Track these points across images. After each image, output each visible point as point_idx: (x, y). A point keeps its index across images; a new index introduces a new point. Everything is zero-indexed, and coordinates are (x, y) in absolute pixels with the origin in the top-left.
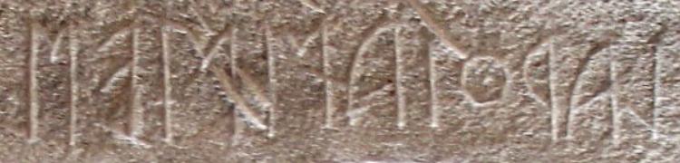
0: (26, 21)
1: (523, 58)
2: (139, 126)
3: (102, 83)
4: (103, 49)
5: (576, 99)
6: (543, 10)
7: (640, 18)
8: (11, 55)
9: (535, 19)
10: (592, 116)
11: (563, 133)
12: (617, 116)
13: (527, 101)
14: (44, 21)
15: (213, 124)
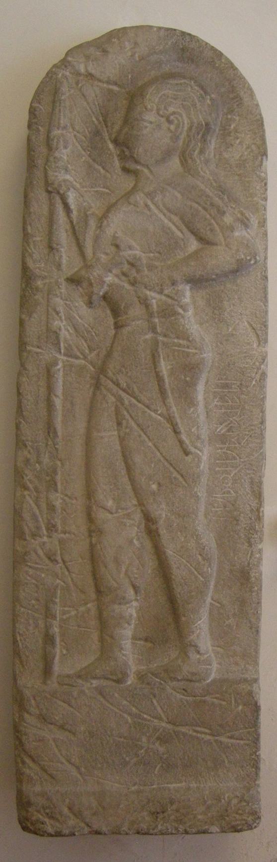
3: (227, 397)
9: (239, 492)
14: (241, 384)
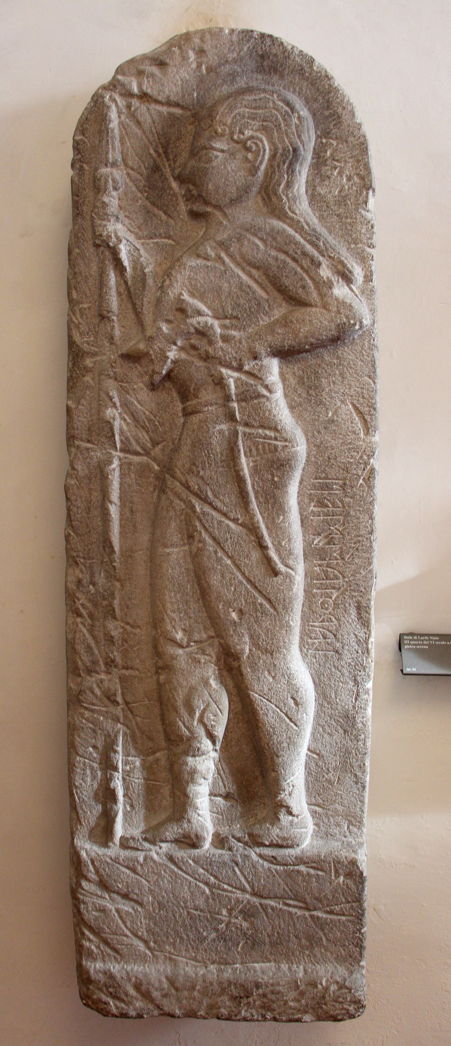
0: (345, 479)
1: (332, 615)
2: (315, 509)
3: (327, 500)
4: (337, 500)
5: (321, 629)
6: (345, 621)
7: (343, 648)
8: (336, 475)
9: (343, 619)
10: (317, 634)
11: (312, 626)
12: (316, 641)
13: (321, 616)
15: (316, 530)
